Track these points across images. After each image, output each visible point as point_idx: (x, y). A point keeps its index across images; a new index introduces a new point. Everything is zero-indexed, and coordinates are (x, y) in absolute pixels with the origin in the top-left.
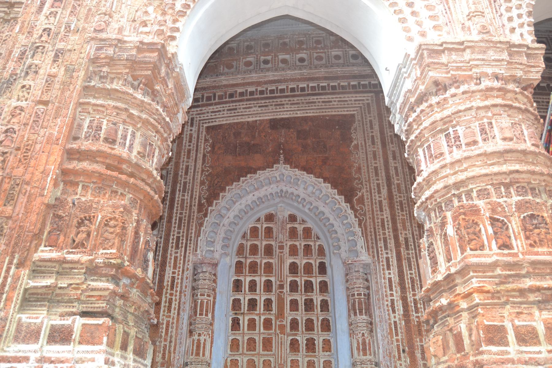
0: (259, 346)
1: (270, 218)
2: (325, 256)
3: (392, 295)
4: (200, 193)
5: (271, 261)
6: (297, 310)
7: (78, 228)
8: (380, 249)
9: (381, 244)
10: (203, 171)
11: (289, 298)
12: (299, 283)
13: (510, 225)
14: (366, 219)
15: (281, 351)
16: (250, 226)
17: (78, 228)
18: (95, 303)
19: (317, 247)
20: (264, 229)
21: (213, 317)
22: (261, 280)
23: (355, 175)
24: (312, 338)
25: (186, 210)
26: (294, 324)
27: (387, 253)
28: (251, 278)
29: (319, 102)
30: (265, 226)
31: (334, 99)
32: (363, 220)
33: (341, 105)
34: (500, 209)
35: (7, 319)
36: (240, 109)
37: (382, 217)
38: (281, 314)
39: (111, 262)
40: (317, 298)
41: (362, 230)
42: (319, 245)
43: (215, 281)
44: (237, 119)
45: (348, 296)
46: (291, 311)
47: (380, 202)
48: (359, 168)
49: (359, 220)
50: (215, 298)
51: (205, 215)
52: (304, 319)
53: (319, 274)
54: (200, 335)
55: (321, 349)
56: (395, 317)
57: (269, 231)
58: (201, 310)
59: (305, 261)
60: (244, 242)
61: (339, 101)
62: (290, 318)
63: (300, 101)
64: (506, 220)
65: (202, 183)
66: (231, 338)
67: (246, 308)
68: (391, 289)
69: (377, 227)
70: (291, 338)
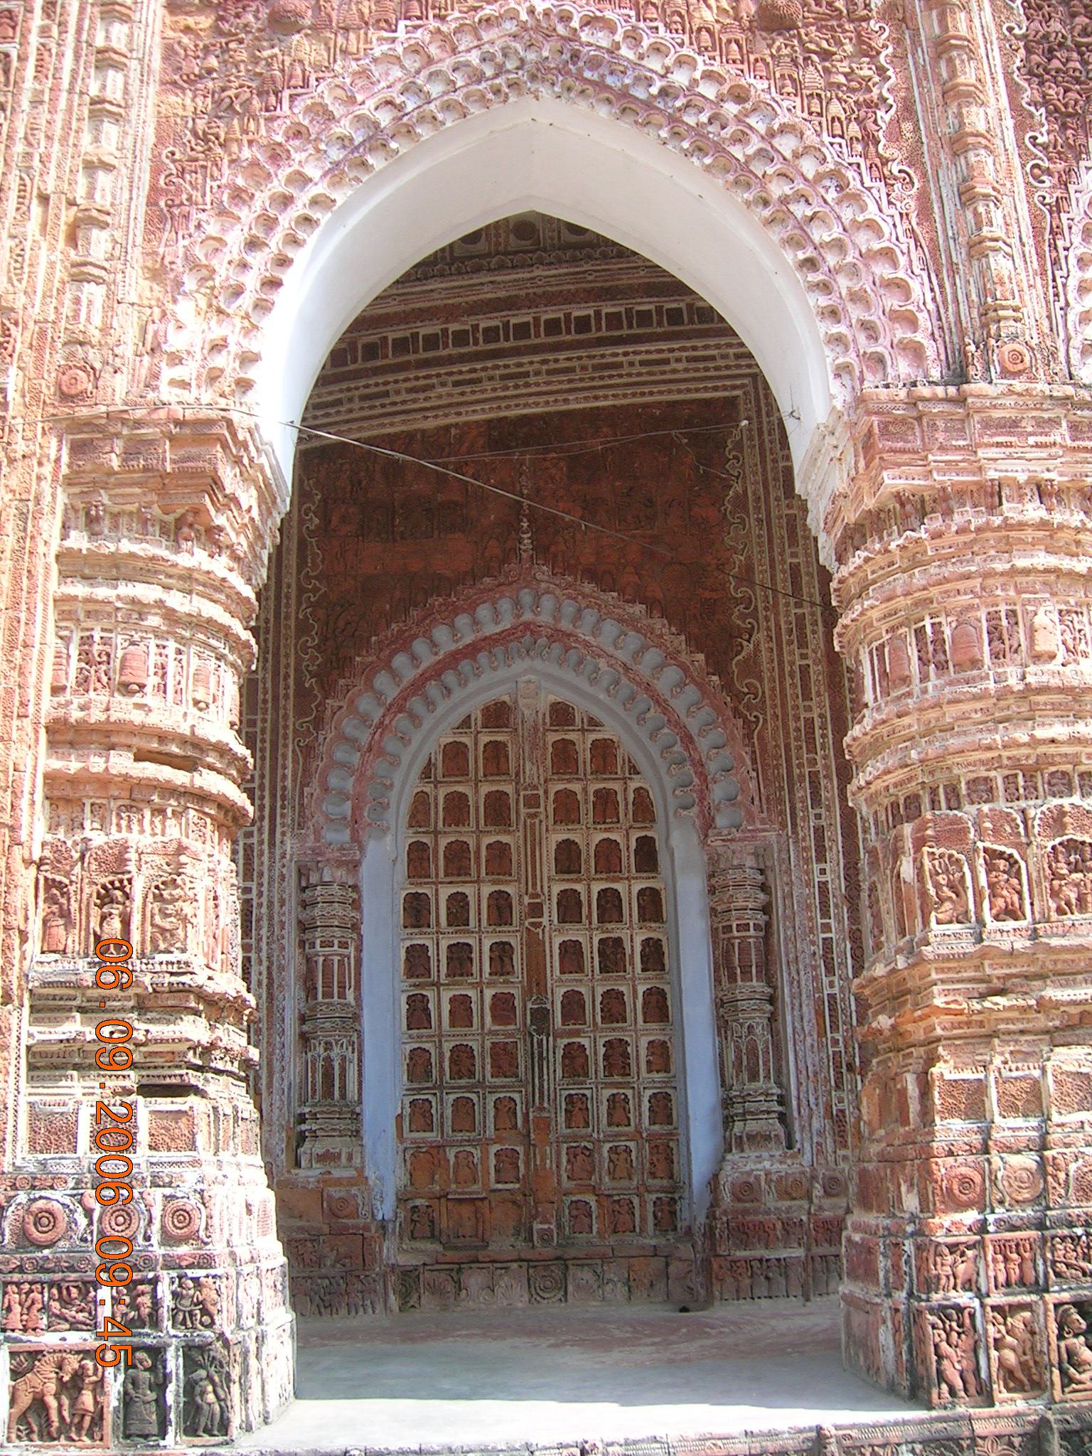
0: (484, 1067)
1: (498, 715)
2: (653, 821)
3: (827, 928)
4: (299, 661)
5: (505, 839)
6: (580, 969)
7: (101, 907)
8: (799, 805)
9: (803, 791)
10: (301, 590)
11: (557, 941)
12: (583, 898)
13: (1023, 864)
14: (765, 721)
15: (541, 1077)
19: (631, 797)
20: (481, 748)
21: (358, 998)
22: (479, 893)
23: (736, 589)
25: (265, 711)
26: (574, 1004)
27: (818, 816)
29: (631, 364)
30: (485, 739)
31: (677, 354)
33: (697, 370)
34: (1008, 829)
36: (398, 392)
37: (808, 715)
38: (536, 981)
40: (634, 937)
42: (637, 790)
43: (356, 905)
44: (392, 424)
45: (714, 932)
46: (562, 972)
47: (804, 670)
48: (749, 569)
49: (747, 723)
50: (359, 949)
51: (319, 723)
52: (600, 991)
54: (328, 1047)
55: (643, 1066)
56: (831, 985)
57: (496, 752)
58: (328, 984)
60: (428, 789)
61: (689, 360)
62: (560, 992)
63: (575, 363)
64: (1017, 856)
65: (303, 628)
66: (408, 1048)
67: (444, 970)
68: (825, 913)
70: (566, 1041)
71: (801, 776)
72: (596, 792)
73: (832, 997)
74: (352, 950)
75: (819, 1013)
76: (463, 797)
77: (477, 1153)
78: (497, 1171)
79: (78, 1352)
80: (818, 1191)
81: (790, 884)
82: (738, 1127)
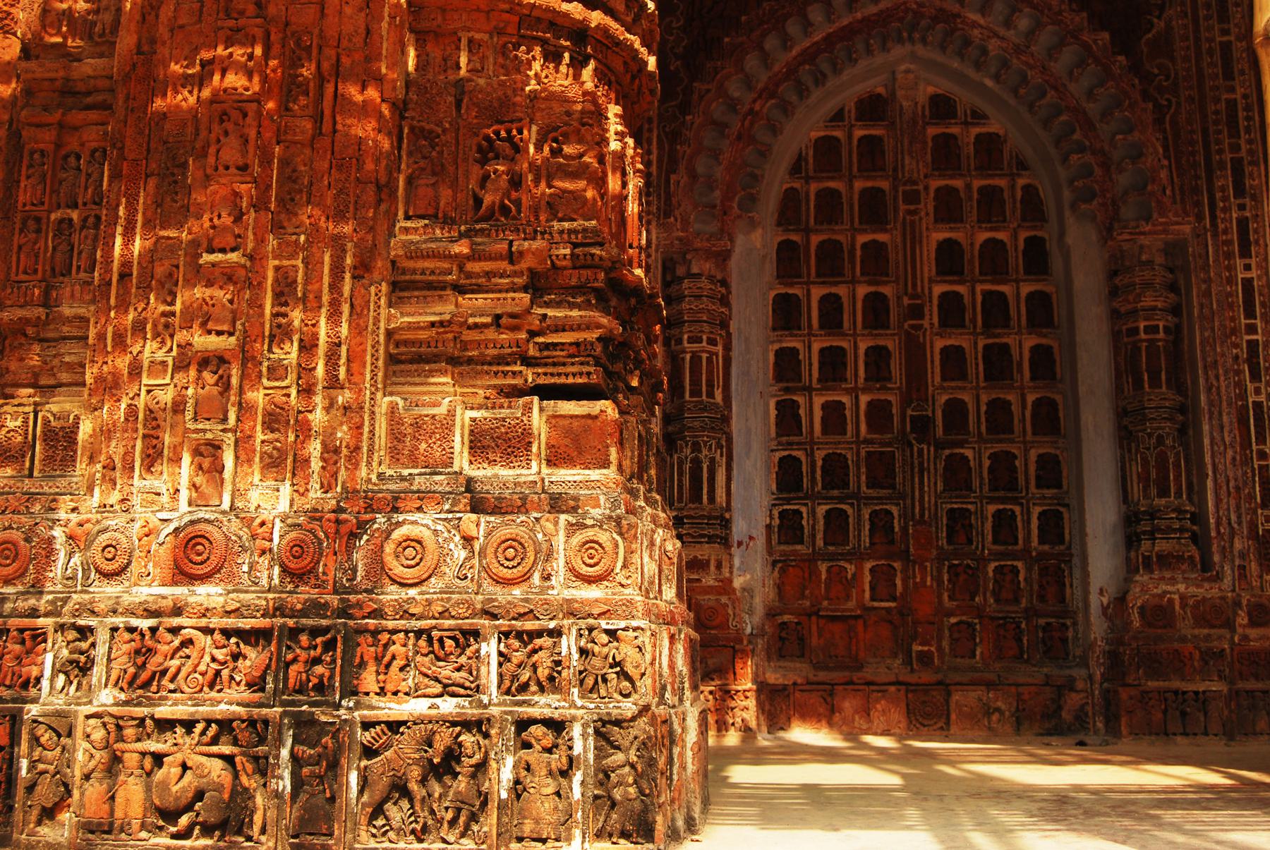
0: (859, 479)
1: (872, 108)
2: (1046, 221)
3: (1252, 329)
5: (882, 237)
6: (963, 376)
8: (1219, 195)
9: (1225, 180)
11: (939, 344)
12: (967, 300)
14: (1178, 104)
15: (921, 489)
16: (815, 135)
17: (483, 161)
18: (564, 364)
19: (1019, 194)
20: (855, 142)
24: (1008, 453)
27: (1242, 207)
28: (824, 291)
32: (1169, 106)
35: (362, 408)
39: (593, 255)
40: (1023, 344)
41: (1166, 138)
42: (1026, 188)
43: (725, 301)
45: (1116, 336)
46: (944, 379)
50: (728, 348)
52: (984, 398)
53: (1027, 272)
54: (696, 448)
58: (695, 382)
59: (983, 236)
68: (1250, 313)
69: (1212, 129)
70: (947, 452)
71: (1222, 165)
72: (981, 190)
73: (1258, 405)
74: (720, 348)
75: (1243, 422)
76: (834, 193)
77: (851, 569)
78: (872, 588)
79: (454, 724)
80: (1242, 619)
81: (1208, 281)
82: (1145, 545)
